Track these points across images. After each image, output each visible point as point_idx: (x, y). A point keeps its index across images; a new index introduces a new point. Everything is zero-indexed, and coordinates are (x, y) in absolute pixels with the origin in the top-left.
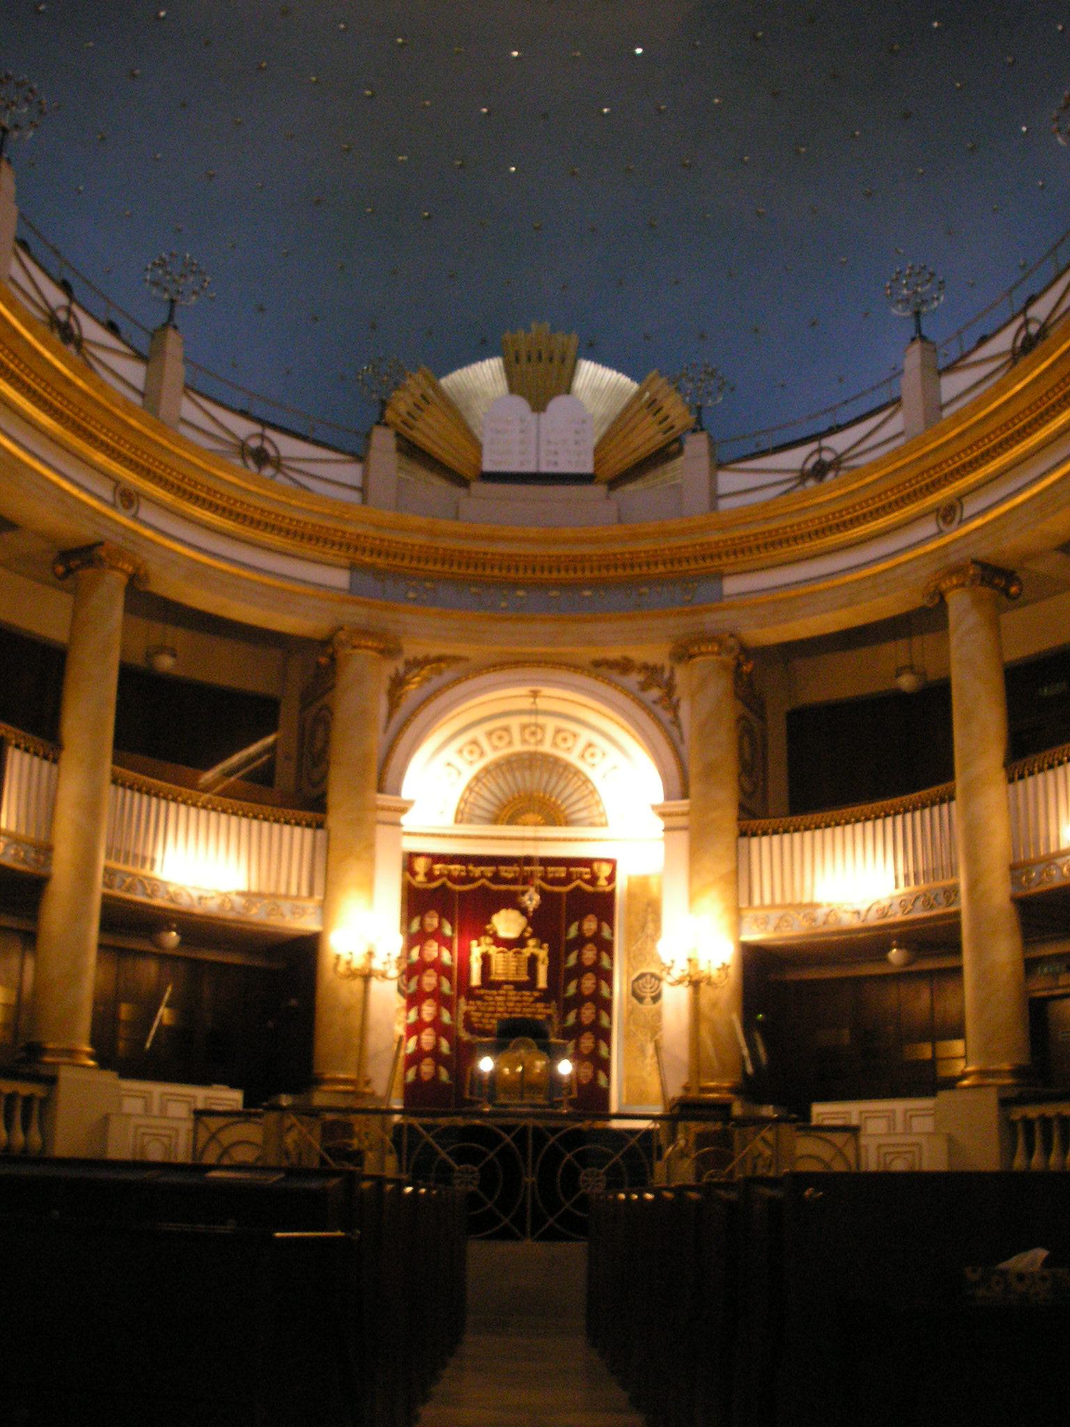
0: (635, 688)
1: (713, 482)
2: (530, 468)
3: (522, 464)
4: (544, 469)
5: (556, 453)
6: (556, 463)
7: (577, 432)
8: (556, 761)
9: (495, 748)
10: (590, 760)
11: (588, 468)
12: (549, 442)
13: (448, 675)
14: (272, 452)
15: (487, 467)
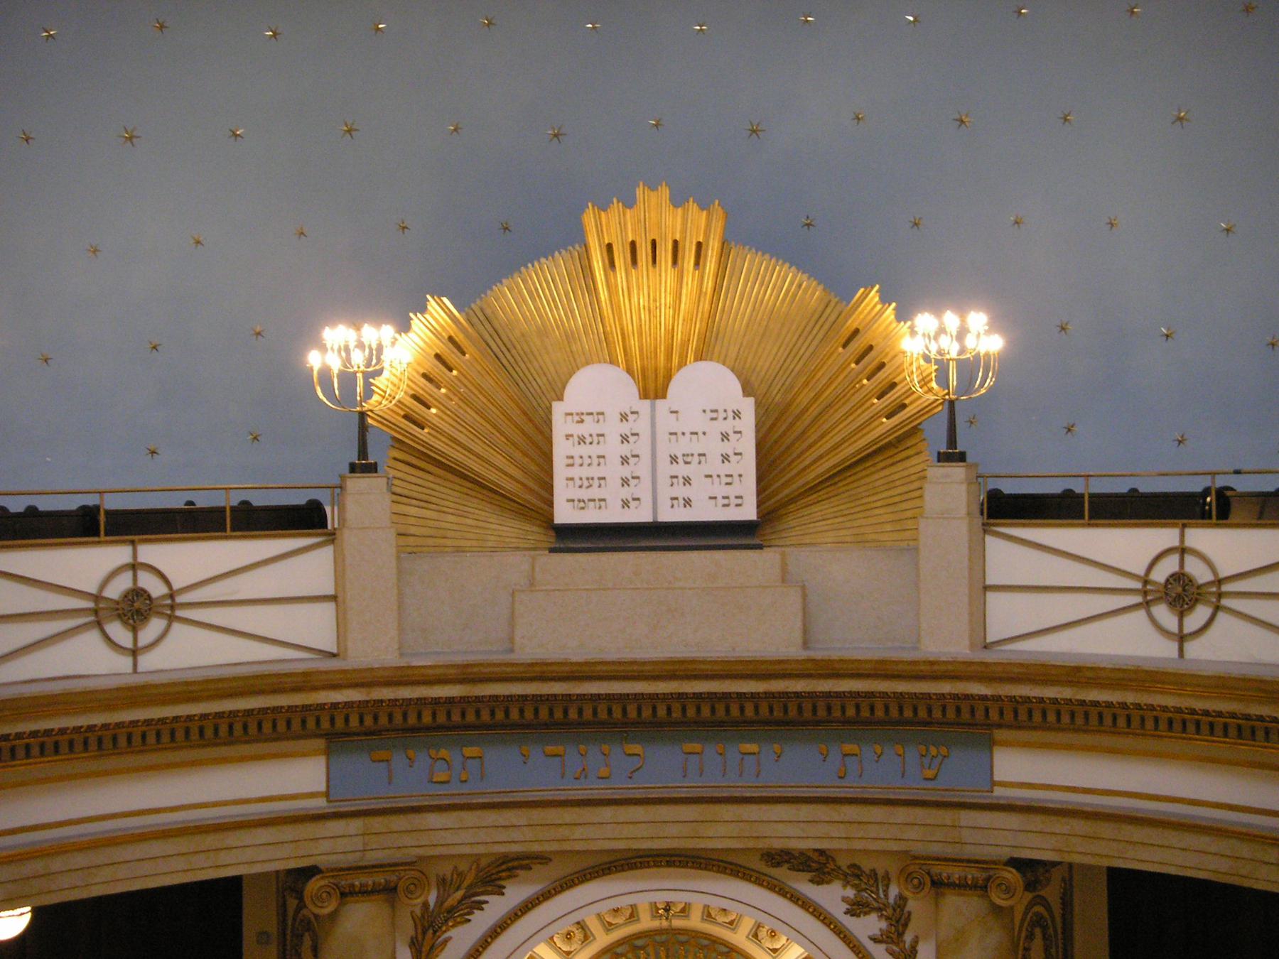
0: (838, 910)
1: (978, 557)
2: (641, 514)
3: (625, 504)
4: (669, 515)
5: (687, 481)
6: (688, 502)
7: (725, 437)
8: (715, 941)
9: (609, 927)
10: (768, 944)
11: (748, 512)
12: (674, 459)
13: (516, 893)
14: (156, 588)
15: (564, 514)
